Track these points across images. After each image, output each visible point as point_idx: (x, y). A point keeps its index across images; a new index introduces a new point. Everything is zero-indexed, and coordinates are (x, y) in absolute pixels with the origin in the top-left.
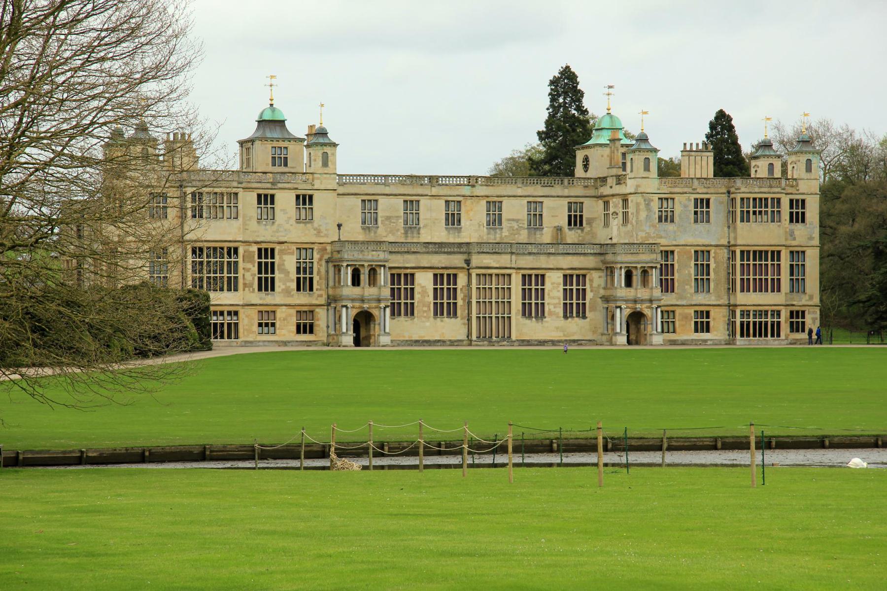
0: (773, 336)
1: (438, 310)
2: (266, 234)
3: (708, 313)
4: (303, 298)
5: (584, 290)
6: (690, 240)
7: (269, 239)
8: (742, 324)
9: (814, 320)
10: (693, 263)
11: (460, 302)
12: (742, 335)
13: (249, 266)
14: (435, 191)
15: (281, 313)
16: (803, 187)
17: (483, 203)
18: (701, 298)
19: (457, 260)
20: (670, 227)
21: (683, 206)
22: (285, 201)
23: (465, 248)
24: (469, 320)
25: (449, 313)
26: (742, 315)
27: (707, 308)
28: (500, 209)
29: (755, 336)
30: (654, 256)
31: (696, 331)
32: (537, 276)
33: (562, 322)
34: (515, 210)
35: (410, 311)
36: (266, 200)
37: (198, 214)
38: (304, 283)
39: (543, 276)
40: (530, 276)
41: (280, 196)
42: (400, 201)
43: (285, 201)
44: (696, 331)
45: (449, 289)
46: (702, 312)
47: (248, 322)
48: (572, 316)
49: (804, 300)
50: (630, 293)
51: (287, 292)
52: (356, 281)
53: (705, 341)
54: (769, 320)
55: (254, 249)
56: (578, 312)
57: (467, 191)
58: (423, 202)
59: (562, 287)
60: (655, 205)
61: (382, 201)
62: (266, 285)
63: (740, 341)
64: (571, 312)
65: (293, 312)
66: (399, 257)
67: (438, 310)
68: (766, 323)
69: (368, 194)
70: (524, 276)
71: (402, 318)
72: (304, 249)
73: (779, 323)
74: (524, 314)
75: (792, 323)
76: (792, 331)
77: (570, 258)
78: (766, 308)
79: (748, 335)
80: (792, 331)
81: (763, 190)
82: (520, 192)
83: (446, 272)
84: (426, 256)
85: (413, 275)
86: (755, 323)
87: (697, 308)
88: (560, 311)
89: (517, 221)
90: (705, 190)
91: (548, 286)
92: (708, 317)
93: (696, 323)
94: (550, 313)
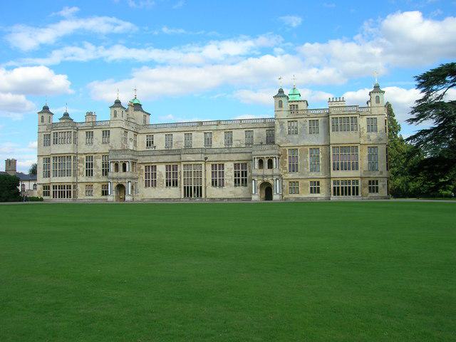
0: (353, 194)
1: (168, 184)
2: (89, 149)
3: (318, 182)
4: (104, 179)
5: (246, 172)
6: (307, 143)
7: (90, 151)
8: (334, 188)
9: (383, 186)
10: (308, 155)
11: (179, 180)
12: (334, 195)
13: (80, 164)
14: (198, 129)
15: (95, 186)
16: (375, 111)
17: (223, 133)
18: (313, 174)
19: (176, 158)
20: (295, 137)
21: (303, 124)
22: (98, 134)
23: (178, 152)
24: (180, 187)
25: (173, 185)
26: (334, 183)
27: (318, 180)
28: (232, 135)
29: (342, 194)
30: (274, 151)
31: (311, 192)
32: (219, 165)
33: (233, 189)
34: (239, 136)
35: (154, 185)
36: (90, 135)
37: (56, 142)
38: (105, 172)
39: (223, 165)
40: (216, 165)
41: (95, 131)
42: (183, 134)
43: (98, 134)
44: (311, 192)
45: (173, 173)
46: (315, 182)
47: (81, 189)
48: (239, 186)
49: (377, 174)
50: (260, 172)
51: (98, 176)
52: (117, 169)
53: (317, 198)
54: (351, 186)
55: (84, 157)
56: (242, 183)
57: (214, 128)
58: (194, 133)
59: (233, 170)
60: (286, 125)
61: (174, 134)
62: (89, 173)
63: (333, 198)
64: (239, 182)
65: (100, 185)
66: (149, 158)
67: (168, 184)
68: (349, 187)
69: (169, 130)
70: (212, 165)
71: (150, 188)
72: (105, 156)
73: (357, 187)
74: (213, 185)
75: (370, 187)
76: (370, 192)
77: (238, 154)
78: (349, 179)
79: (338, 195)
80: (370, 192)
81: (346, 113)
82: (241, 127)
83: (172, 164)
84: (161, 157)
85: (155, 166)
86: (342, 187)
87: (312, 180)
88: (233, 183)
89: (240, 141)
90: (315, 116)
91: (225, 170)
92: (318, 184)
93: (311, 188)
94: (227, 184)
